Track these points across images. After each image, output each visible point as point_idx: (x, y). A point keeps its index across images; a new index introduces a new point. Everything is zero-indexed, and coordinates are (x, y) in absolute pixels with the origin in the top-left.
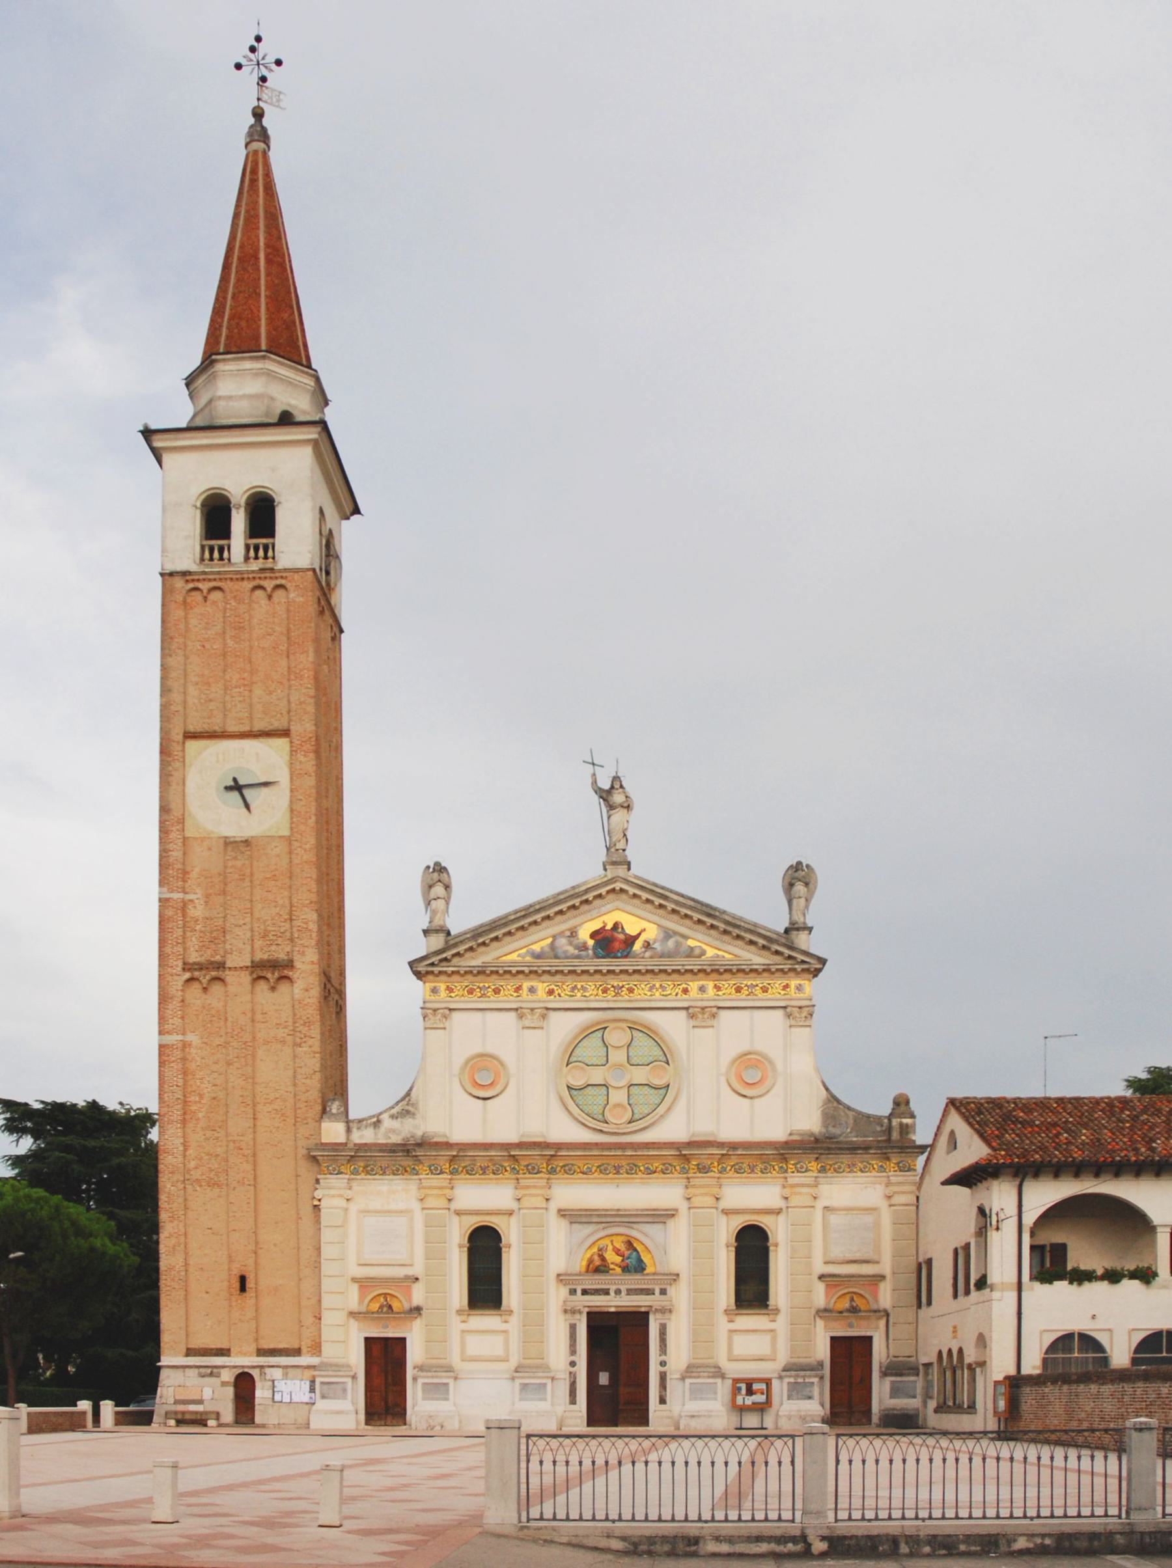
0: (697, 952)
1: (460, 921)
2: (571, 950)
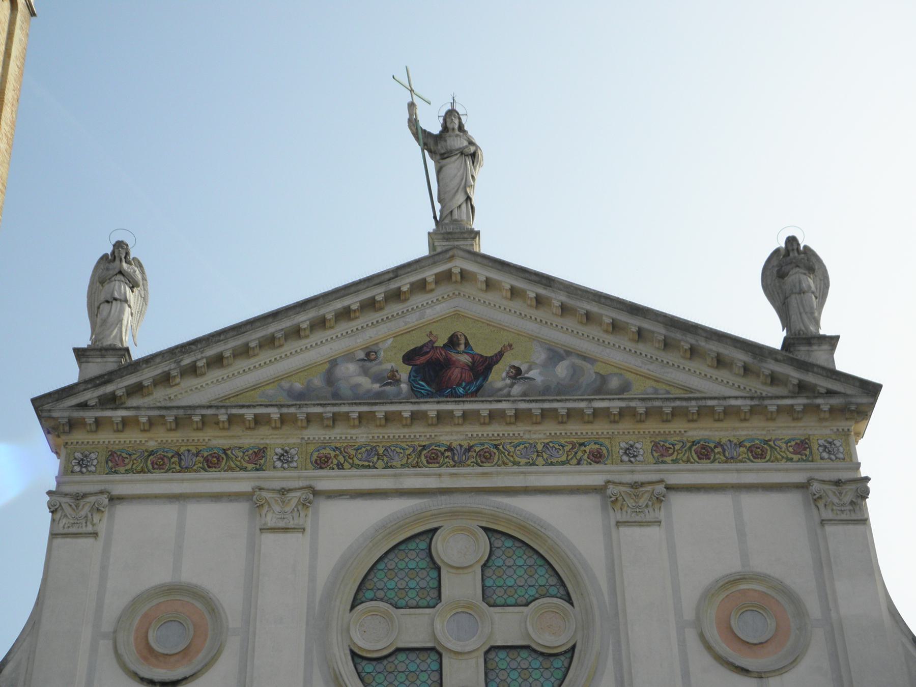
0: (614, 383)
1: (148, 331)
2: (366, 383)
